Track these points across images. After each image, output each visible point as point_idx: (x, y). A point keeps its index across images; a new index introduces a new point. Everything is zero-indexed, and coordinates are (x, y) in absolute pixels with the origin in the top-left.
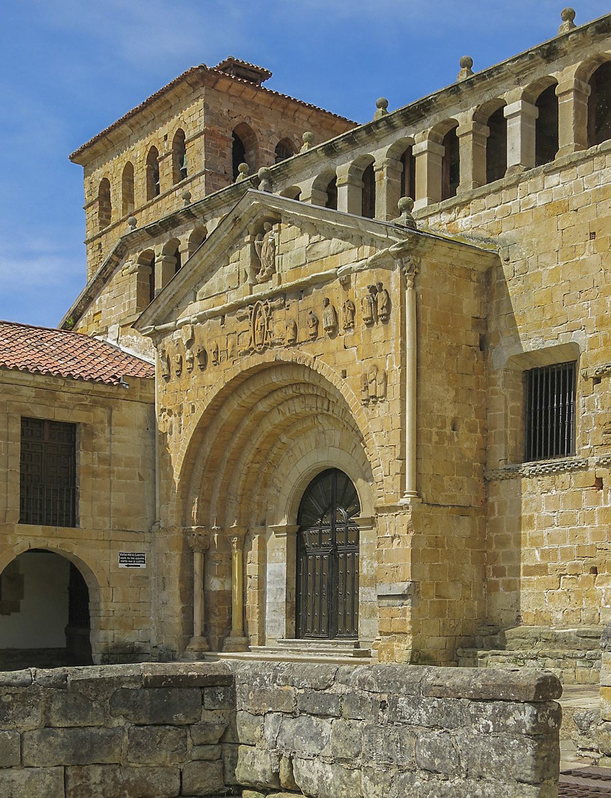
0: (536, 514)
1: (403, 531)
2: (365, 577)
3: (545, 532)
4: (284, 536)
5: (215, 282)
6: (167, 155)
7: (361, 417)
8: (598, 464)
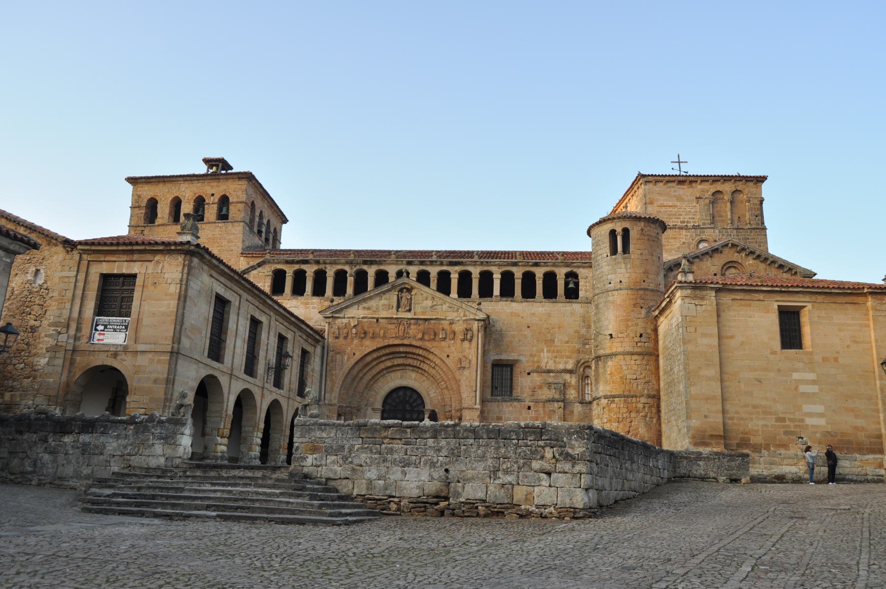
0: (503, 416)
5: (373, 303)
6: (213, 204)
8: (529, 401)
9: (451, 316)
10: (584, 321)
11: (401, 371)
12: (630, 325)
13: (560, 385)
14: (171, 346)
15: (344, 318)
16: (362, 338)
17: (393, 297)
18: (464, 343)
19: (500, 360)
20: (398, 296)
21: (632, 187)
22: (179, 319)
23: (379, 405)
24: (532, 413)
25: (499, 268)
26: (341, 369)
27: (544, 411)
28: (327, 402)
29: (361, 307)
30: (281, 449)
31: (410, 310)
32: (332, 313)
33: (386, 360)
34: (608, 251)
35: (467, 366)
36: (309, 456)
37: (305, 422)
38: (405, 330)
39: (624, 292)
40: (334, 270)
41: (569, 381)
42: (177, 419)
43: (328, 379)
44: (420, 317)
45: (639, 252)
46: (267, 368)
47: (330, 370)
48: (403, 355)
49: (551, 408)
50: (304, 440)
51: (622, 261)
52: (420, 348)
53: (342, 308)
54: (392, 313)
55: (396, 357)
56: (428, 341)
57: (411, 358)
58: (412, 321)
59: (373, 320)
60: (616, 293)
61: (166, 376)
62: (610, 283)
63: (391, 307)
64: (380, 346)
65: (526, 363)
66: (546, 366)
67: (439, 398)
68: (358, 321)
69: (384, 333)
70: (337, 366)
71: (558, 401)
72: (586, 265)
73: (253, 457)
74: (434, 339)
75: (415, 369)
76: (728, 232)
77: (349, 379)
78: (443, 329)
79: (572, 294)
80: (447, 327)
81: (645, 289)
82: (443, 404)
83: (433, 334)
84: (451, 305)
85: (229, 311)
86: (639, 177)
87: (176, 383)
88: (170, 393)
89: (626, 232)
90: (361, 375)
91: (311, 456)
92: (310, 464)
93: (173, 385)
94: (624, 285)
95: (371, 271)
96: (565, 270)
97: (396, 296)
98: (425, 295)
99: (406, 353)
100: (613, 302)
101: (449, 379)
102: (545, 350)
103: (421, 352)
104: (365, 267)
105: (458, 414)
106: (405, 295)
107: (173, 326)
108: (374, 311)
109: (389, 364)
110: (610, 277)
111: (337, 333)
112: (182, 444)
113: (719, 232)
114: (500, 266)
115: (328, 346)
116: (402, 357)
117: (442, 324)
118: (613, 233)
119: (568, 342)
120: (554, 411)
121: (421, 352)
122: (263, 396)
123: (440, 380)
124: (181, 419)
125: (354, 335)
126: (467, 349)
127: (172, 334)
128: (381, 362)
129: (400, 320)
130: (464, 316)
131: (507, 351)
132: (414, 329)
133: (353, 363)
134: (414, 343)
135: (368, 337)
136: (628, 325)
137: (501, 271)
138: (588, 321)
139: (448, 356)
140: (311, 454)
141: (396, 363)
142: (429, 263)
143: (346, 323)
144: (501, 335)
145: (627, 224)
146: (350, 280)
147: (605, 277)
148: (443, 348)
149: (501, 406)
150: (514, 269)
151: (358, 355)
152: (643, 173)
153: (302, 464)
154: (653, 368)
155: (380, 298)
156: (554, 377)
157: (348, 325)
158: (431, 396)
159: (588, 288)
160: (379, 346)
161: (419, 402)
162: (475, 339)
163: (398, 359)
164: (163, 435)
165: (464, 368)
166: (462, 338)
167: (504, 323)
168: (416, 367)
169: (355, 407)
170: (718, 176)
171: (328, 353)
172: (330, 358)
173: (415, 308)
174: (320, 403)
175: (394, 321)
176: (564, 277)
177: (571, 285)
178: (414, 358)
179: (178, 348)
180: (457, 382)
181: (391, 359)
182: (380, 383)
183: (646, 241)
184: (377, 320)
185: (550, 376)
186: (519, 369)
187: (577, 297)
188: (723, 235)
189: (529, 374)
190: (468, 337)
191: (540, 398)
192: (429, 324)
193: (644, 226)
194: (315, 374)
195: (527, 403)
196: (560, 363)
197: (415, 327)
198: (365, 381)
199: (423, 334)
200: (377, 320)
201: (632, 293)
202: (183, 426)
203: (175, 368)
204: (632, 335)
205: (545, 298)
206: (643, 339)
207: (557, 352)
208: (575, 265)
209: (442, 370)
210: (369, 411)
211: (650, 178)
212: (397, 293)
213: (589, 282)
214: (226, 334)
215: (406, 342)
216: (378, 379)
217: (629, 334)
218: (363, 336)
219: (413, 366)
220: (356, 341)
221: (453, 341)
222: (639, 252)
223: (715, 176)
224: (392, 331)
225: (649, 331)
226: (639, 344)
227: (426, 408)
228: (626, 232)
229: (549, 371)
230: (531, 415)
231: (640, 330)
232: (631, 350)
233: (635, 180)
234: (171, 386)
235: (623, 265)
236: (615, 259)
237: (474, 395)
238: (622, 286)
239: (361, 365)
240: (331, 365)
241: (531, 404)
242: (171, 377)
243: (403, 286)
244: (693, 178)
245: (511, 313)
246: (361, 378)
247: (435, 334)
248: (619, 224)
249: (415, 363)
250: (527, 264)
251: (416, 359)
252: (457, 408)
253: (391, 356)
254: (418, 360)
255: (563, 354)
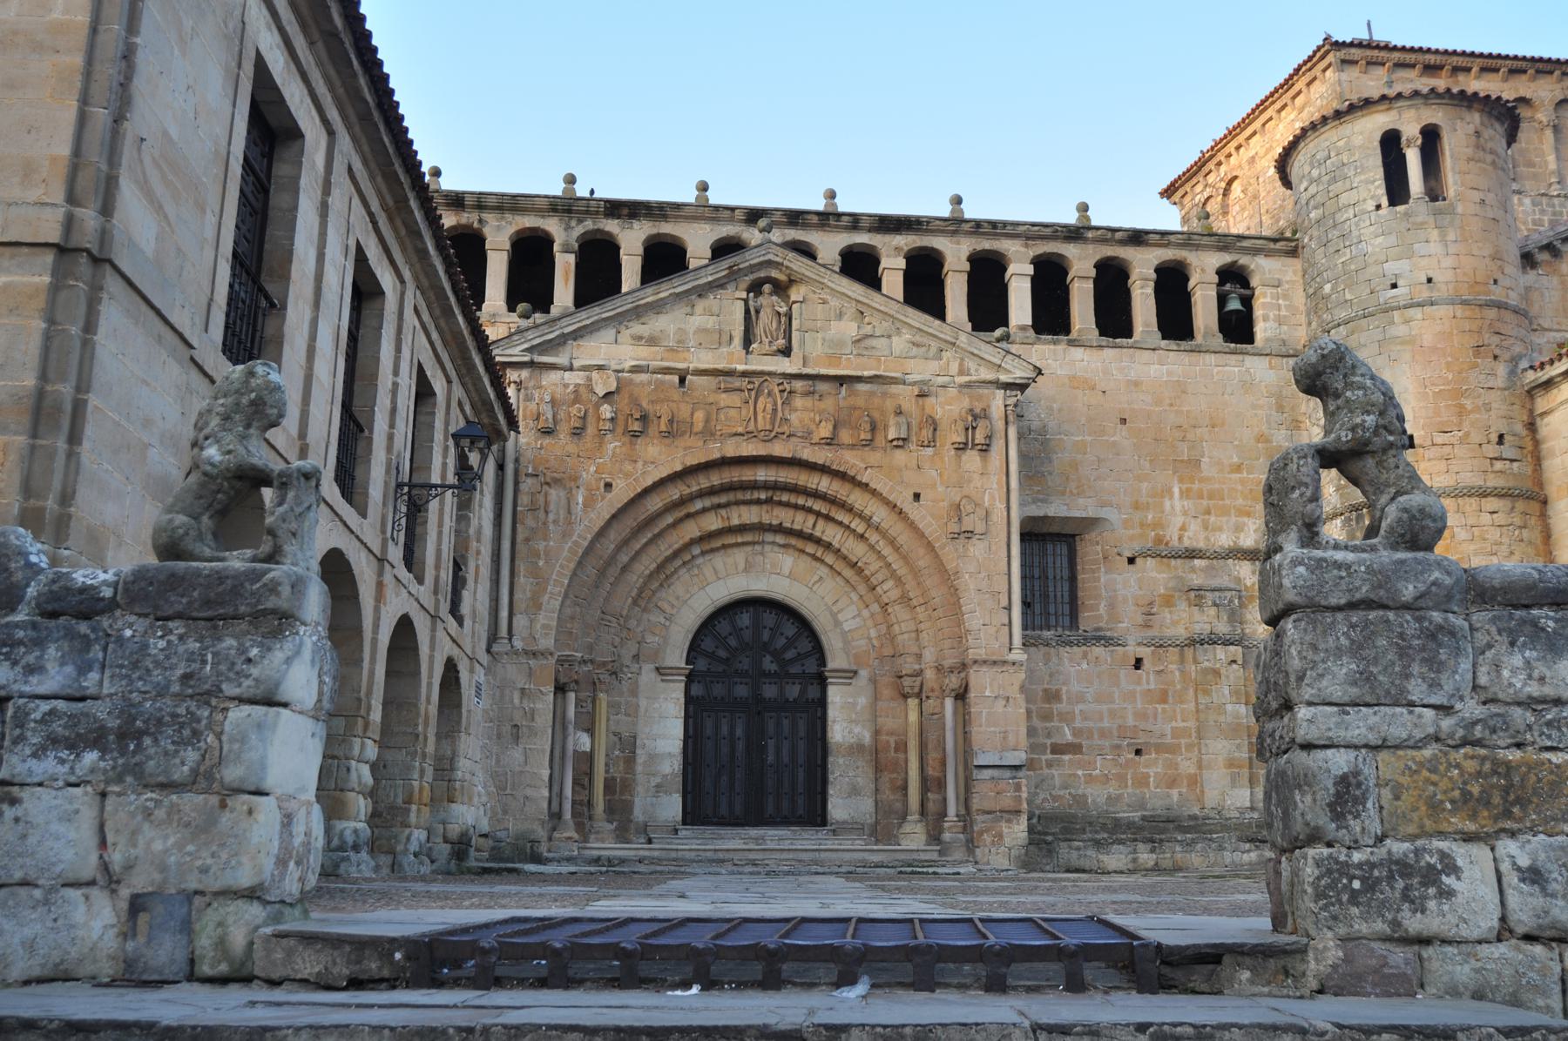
0: (1064, 689)
1: (1014, 691)
2: (840, 745)
3: (1078, 708)
4: (681, 681)
5: (665, 324)
7: (949, 553)
8: (1139, 644)
9: (921, 370)
10: (1280, 408)
11: (749, 549)
12: (1469, 407)
13: (1228, 594)
14: (60, 214)
15: (571, 369)
16: (635, 435)
17: (730, 307)
18: (964, 458)
19: (1046, 518)
20: (747, 311)
21: (1288, 83)
22: (107, 72)
23: (676, 657)
24: (1148, 679)
25: (1027, 246)
26: (565, 535)
27: (1182, 672)
28: (518, 644)
29: (626, 334)
30: (414, 807)
31: (786, 352)
32: (529, 350)
33: (704, 510)
34: (1382, 191)
35: (980, 528)
36: (1461, 853)
37: (1382, 578)
38: (775, 411)
39: (1443, 311)
40: (512, 230)
41: (1249, 584)
42: (220, 577)
43: (522, 567)
44: (823, 371)
45: (1477, 196)
46: (393, 484)
47: (527, 540)
48: (763, 496)
49: (1206, 664)
50: (1398, 725)
51: (1431, 220)
52: (823, 469)
53: (563, 335)
54: (732, 357)
55: (738, 503)
56: (853, 447)
57: (787, 505)
58: (798, 385)
59: (667, 377)
60: (1416, 313)
61: (30, 381)
62: (1394, 286)
63: (725, 338)
64: (695, 462)
65: (1122, 531)
66: (1180, 539)
67: (873, 633)
68: (618, 379)
69: (707, 421)
70: (551, 527)
71: (1227, 643)
72: (1279, 245)
73: (350, 839)
74: (869, 443)
75: (793, 541)
76: (1553, 206)
77: (591, 571)
78: (899, 413)
79: (1238, 328)
80: (909, 404)
81: (1500, 306)
82: (888, 651)
83: (868, 427)
84: (918, 338)
85: (296, 179)
86: (1327, 47)
87: (89, 431)
88: (57, 484)
89: (1431, 137)
90: (624, 558)
91: (1481, 852)
92: (1488, 922)
93: (74, 438)
94: (1442, 290)
95: (631, 241)
96: (1216, 260)
97: (742, 303)
98: (834, 303)
99: (775, 487)
100: (1410, 341)
101: (915, 572)
102: (1176, 490)
103: (824, 484)
104: (611, 226)
105: (954, 681)
106: (768, 302)
107: (74, 105)
108: (671, 350)
109: (713, 522)
110: (1392, 267)
111: (550, 416)
112: (270, 782)
113: (1534, 204)
114: (1028, 238)
115: (517, 460)
116: (758, 502)
117: (893, 396)
118: (1391, 143)
119: (1238, 468)
120: (1217, 673)
121: (824, 484)
122: (379, 597)
123: (880, 577)
124: (256, 576)
125: (608, 425)
126: (976, 476)
127: (64, 150)
128: (689, 516)
129: (757, 381)
130: (961, 372)
131: (1063, 493)
132: (805, 409)
133: (608, 517)
134: (807, 454)
135: (652, 430)
136: (1462, 406)
137: (1031, 254)
138: (1293, 409)
139: (917, 496)
140: (1468, 838)
141: (735, 521)
142: (815, 219)
143: (577, 385)
144: (1045, 443)
145: (1435, 115)
146: (565, 266)
147: (1372, 270)
148: (900, 470)
149: (1055, 660)
150: (1070, 251)
151: (623, 491)
152: (1339, 37)
153: (1414, 924)
154: (1534, 534)
155: (688, 309)
156: (1205, 570)
157: (582, 390)
158: (846, 627)
159: (1283, 313)
160: (692, 460)
161: (805, 645)
162: (997, 445)
163: (744, 509)
164: (100, 711)
165: (969, 534)
166: (961, 439)
167: (1051, 408)
168: (800, 534)
169: (604, 664)
170: (1524, 58)
171: (516, 483)
172: (524, 499)
173: (802, 342)
174: (495, 648)
175: (737, 383)
176: (1216, 279)
177: (1234, 305)
178: (796, 507)
179: (104, 236)
180: (948, 579)
181: (719, 506)
182: (678, 588)
183: (1490, 168)
184: (682, 381)
185: (1193, 569)
186: (1099, 548)
187: (1249, 338)
188: (1543, 212)
189: (1131, 561)
190: (980, 437)
191: (1169, 632)
192: (852, 393)
193: (1482, 124)
194: (482, 549)
195: (1133, 650)
196: (1220, 529)
197: (808, 402)
198: (635, 578)
199: (835, 427)
200: (682, 381)
201: (1468, 313)
202: (276, 634)
203: (87, 345)
204: (1476, 437)
205: (1164, 338)
206: (1507, 450)
207: (1210, 498)
208: (1246, 243)
209: (892, 542)
210: (647, 675)
211: (1353, 50)
212: (744, 295)
213: (1285, 297)
214: (285, 277)
215: (779, 449)
216: (673, 574)
217: (1467, 434)
218: (636, 426)
219: (790, 532)
220: (613, 445)
221: (930, 451)
222: (1477, 196)
223: (1516, 58)
224: (733, 413)
225: (1519, 428)
226: (1499, 465)
227: (831, 665)
228: (1431, 137)
229: (1191, 554)
230: (1145, 687)
231: (1500, 426)
232: (1477, 481)
233: (1310, 58)
234: (62, 445)
235: (1434, 234)
236: (1407, 214)
237: (1007, 622)
238: (1435, 295)
239: (630, 522)
240: (530, 522)
241: (1144, 652)
242: (66, 390)
243: (762, 274)
244: (1461, 59)
245: (1072, 378)
246: (625, 569)
247: (873, 429)
248: (1410, 114)
249: (800, 521)
250: (1109, 235)
251: (803, 508)
252: (947, 663)
253: (723, 499)
254: (810, 510)
255: (1227, 502)
